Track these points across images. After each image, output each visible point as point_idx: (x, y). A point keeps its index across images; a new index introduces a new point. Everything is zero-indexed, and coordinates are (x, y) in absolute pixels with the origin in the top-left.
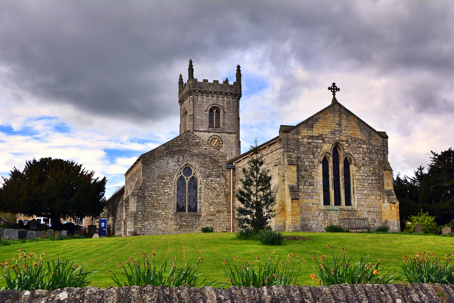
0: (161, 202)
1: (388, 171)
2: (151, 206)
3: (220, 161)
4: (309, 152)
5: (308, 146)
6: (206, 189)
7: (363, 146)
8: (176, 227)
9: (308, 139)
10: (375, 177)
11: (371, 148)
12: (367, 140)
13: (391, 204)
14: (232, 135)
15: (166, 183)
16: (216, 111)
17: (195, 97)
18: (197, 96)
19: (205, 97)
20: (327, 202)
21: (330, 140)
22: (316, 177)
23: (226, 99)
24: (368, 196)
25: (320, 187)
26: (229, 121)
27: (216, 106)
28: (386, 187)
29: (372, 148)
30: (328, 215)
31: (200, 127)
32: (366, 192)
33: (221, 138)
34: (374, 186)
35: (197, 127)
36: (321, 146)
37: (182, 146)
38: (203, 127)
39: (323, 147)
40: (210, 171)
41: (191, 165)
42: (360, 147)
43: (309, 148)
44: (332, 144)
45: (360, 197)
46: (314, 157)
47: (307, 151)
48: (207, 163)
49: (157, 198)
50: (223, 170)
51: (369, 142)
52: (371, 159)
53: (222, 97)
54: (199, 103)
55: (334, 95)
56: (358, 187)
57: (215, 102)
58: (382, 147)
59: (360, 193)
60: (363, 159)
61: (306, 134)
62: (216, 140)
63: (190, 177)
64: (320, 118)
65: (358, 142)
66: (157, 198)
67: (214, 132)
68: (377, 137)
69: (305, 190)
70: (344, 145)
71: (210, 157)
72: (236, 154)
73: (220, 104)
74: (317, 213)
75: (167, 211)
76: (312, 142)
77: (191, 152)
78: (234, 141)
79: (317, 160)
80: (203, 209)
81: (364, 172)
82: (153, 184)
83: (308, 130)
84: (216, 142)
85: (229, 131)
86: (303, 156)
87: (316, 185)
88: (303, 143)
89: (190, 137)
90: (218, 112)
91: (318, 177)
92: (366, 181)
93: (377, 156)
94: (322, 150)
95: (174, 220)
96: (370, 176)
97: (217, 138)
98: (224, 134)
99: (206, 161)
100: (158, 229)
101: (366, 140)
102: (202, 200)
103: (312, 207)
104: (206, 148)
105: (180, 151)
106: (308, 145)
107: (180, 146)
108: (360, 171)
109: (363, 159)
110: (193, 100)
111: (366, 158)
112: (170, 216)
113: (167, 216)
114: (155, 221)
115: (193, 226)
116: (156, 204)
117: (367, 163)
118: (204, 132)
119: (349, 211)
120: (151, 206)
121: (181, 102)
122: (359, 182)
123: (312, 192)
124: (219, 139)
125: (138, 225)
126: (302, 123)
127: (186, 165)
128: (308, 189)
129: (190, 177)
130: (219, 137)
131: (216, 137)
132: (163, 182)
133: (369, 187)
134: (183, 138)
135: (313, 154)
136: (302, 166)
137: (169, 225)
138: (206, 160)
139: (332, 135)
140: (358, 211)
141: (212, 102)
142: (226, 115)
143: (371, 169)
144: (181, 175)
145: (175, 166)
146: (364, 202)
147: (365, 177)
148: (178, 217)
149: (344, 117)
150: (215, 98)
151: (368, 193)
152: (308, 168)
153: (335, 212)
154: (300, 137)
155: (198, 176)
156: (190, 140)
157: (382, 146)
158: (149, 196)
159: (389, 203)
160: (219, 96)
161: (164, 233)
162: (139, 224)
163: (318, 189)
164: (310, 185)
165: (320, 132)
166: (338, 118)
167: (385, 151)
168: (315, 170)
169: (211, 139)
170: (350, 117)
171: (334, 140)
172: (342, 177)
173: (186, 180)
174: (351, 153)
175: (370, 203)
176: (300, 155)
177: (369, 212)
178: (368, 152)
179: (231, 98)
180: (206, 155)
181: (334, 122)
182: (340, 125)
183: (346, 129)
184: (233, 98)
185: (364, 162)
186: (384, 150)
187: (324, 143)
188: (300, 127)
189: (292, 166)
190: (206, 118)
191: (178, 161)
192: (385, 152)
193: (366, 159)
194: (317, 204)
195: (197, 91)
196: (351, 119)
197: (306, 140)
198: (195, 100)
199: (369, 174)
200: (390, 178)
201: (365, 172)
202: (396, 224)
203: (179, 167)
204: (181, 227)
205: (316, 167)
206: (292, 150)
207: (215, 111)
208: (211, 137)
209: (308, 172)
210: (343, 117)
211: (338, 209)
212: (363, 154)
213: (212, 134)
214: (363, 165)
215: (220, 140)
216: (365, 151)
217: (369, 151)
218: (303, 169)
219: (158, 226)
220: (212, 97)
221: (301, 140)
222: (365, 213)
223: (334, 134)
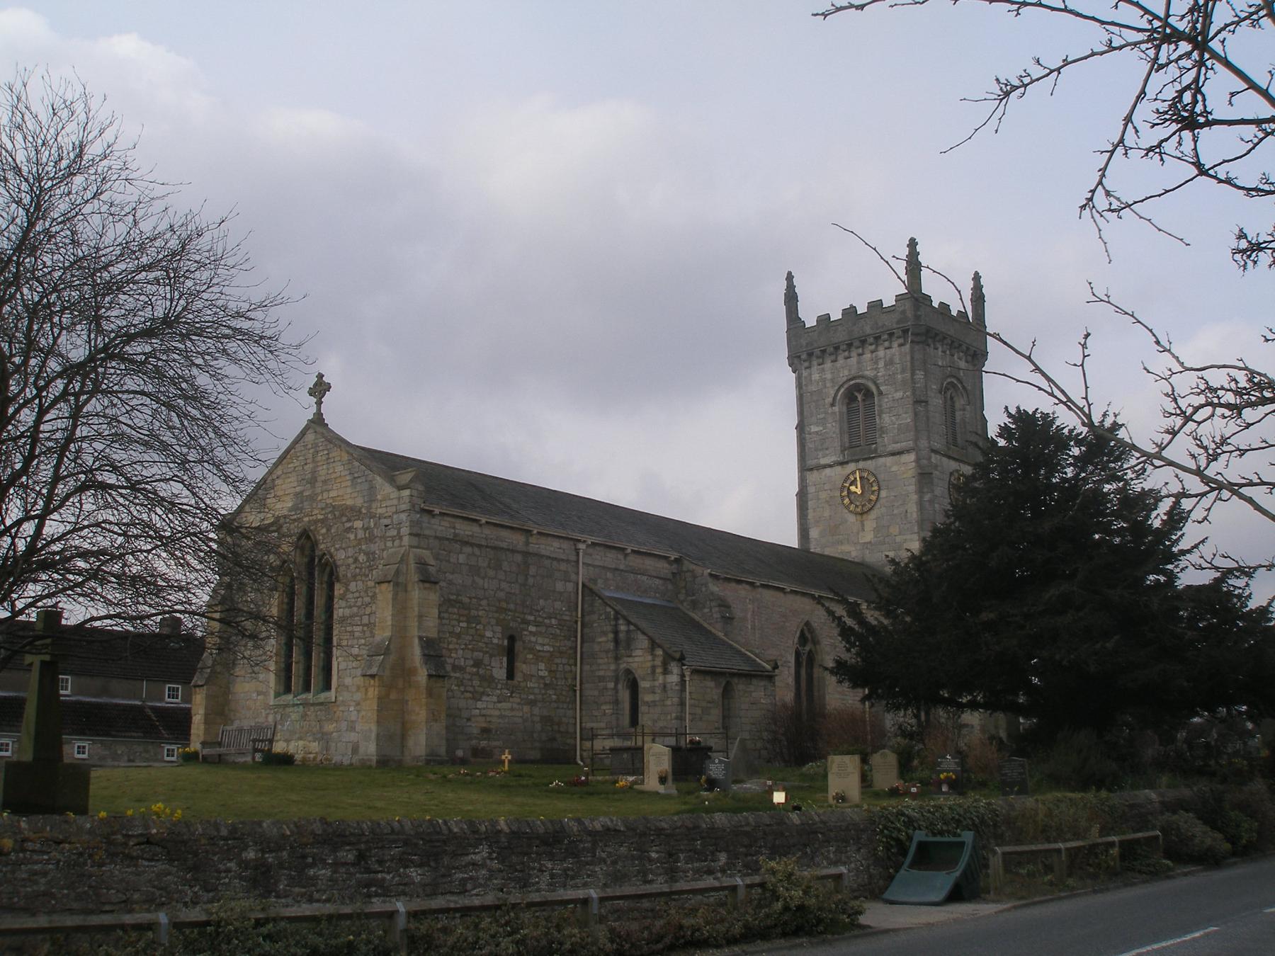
11: (372, 524)
18: (809, 367)
26: (893, 418)
27: (858, 381)
31: (820, 454)
53: (872, 352)
54: (814, 388)
58: (395, 516)
67: (857, 461)
73: (867, 373)
78: (910, 474)
81: (357, 594)
85: (898, 447)
90: (868, 394)
98: (882, 460)
109: (356, 560)
118: (830, 466)
140: (338, 703)
141: (846, 373)
142: (886, 400)
150: (854, 360)
178: (366, 538)
213: (852, 467)
216: (359, 537)
222: (352, 709)
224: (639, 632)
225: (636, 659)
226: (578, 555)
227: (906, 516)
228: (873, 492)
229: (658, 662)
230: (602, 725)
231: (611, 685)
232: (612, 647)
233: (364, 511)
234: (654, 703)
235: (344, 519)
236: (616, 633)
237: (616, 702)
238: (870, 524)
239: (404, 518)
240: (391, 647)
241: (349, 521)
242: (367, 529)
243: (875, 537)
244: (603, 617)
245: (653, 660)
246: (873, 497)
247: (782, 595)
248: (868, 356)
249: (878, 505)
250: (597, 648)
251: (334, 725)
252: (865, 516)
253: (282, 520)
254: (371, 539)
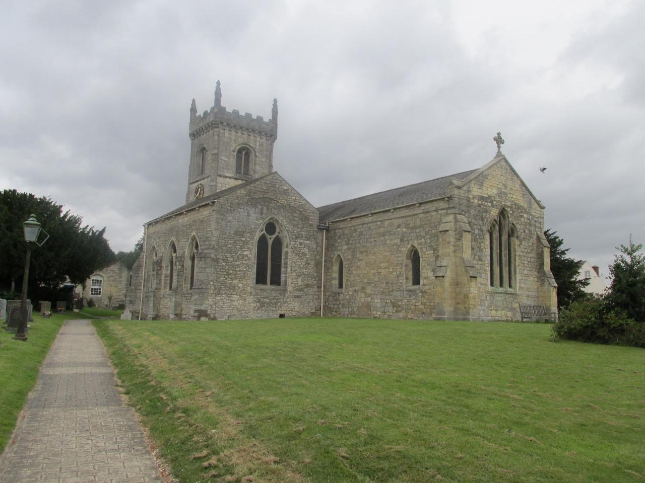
0: (238, 269)
2: (225, 273)
3: (311, 218)
6: (294, 254)
8: (255, 305)
15: (245, 243)
16: (246, 153)
17: (222, 131)
18: (225, 130)
19: (233, 133)
23: (258, 139)
27: (247, 146)
31: (225, 171)
32: (525, 272)
37: (266, 193)
38: (229, 171)
40: (299, 230)
41: (277, 220)
45: (521, 278)
48: (296, 219)
49: (233, 263)
50: (314, 231)
55: (499, 147)
57: (246, 141)
63: (274, 236)
66: (233, 263)
71: (300, 211)
73: (251, 145)
75: (246, 283)
77: (277, 202)
80: (289, 281)
82: (229, 242)
89: (277, 181)
95: (254, 295)
99: (295, 217)
100: (233, 307)
102: (289, 269)
104: (296, 199)
105: (264, 199)
107: (264, 192)
108: (522, 246)
109: (524, 232)
110: (219, 135)
112: (249, 289)
113: (245, 289)
114: (229, 296)
115: (276, 304)
116: (231, 272)
118: (230, 178)
120: (225, 273)
121: (194, 135)
123: (481, 269)
125: (209, 301)
127: (271, 219)
128: (477, 264)
129: (274, 236)
132: (242, 241)
134: (268, 182)
135: (483, 220)
137: (248, 302)
138: (295, 215)
144: (262, 233)
145: (257, 220)
148: (259, 291)
155: (284, 235)
156: (277, 186)
158: (223, 260)
160: (250, 134)
161: (240, 313)
162: (210, 300)
173: (268, 239)
179: (264, 138)
180: (295, 208)
184: (267, 140)
190: (233, 161)
191: (262, 213)
195: (225, 124)
197: (476, 201)
198: (221, 135)
203: (262, 221)
204: (263, 305)
206: (463, 213)
207: (244, 153)
219: (234, 303)
220: (242, 134)
221: (472, 201)
241: (521, 212)
248: (252, 137)
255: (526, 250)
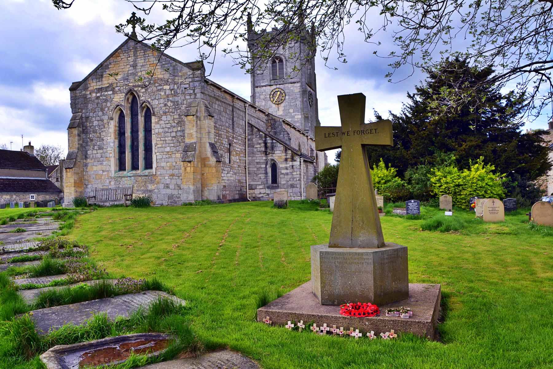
1: (192, 117)
4: (97, 108)
5: (96, 101)
7: (165, 87)
9: (96, 93)
10: (181, 127)
11: (176, 87)
12: (171, 78)
13: (186, 164)
14: (295, 85)
20: (122, 166)
21: (122, 88)
22: (106, 138)
24: (171, 154)
25: (111, 149)
28: (188, 139)
29: (178, 88)
30: (120, 184)
32: (168, 149)
33: (283, 90)
34: (180, 140)
35: (258, 82)
36: (111, 98)
39: (113, 100)
42: (161, 89)
43: (97, 104)
44: (124, 93)
46: (103, 113)
47: (95, 108)
51: (173, 80)
52: (176, 103)
56: (157, 144)
58: (191, 84)
59: (160, 151)
60: (166, 105)
61: (95, 88)
62: (279, 93)
64: (110, 64)
65: (158, 83)
67: (276, 85)
68: (184, 71)
69: (94, 155)
70: (139, 91)
72: (301, 105)
74: (108, 181)
76: (101, 96)
78: (298, 90)
79: (106, 117)
83: (96, 82)
84: (278, 95)
86: (91, 114)
87: (106, 147)
88: (91, 99)
90: (281, 61)
91: (109, 138)
92: (169, 134)
93: (185, 98)
94: (113, 103)
96: (174, 127)
97: (279, 91)
98: (287, 85)
101: (169, 78)
103: (101, 175)
106: (97, 100)
108: (161, 122)
109: (166, 105)
111: (170, 102)
117: (171, 110)
118: (265, 86)
119: (146, 176)
122: (160, 136)
123: (102, 157)
124: (282, 91)
126: (90, 75)
128: (97, 153)
130: (282, 89)
131: (277, 90)
133: (172, 142)
135: (102, 110)
136: (90, 127)
139: (124, 82)
140: (157, 175)
143: (175, 117)
146: (165, 163)
147: (167, 130)
149: (141, 54)
151: (171, 151)
152: (97, 128)
153: (129, 178)
154: (88, 93)
157: (192, 82)
159: (182, 163)
163: (109, 152)
164: (100, 149)
165: (110, 82)
166: (133, 58)
167: (196, 88)
168: (105, 129)
169: (272, 93)
170: (148, 52)
171: (127, 88)
172: (141, 135)
174: (149, 100)
175: (174, 164)
176: (88, 114)
177: (173, 175)
178: (172, 94)
181: (128, 63)
182: (134, 66)
183: (142, 69)
185: (166, 108)
186: (195, 87)
187: (114, 94)
188: (89, 81)
189: (73, 130)
192: (196, 90)
193: (169, 104)
194: (108, 171)
196: (150, 55)
199: (173, 124)
200: (193, 126)
201: (168, 122)
202: (191, 191)
205: (106, 126)
206: (80, 110)
207: (277, 61)
208: (273, 91)
209: (97, 133)
210: (139, 54)
211: (131, 175)
212: (164, 99)
213: (274, 87)
214: (165, 113)
215: (282, 92)
216: (167, 93)
217: (173, 92)
218: (92, 130)
221: (89, 96)
222: (167, 178)
223: (127, 79)
224: (278, 143)
225: (277, 155)
226: (245, 109)
227: (296, 107)
228: (283, 97)
229: (289, 156)
230: (260, 183)
231: (264, 166)
232: (263, 150)
233: (170, 80)
234: (287, 174)
235: (157, 85)
236: (265, 143)
237: (266, 173)
238: (282, 107)
239: (198, 85)
240: (196, 147)
241: (160, 85)
242: (172, 89)
243: (284, 113)
244: (258, 136)
245: (286, 156)
246: (283, 98)
247: (294, 130)
249: (285, 101)
250: (255, 150)
251: (156, 186)
252: (279, 105)
253: (115, 85)
254: (176, 95)
255: (168, 126)
